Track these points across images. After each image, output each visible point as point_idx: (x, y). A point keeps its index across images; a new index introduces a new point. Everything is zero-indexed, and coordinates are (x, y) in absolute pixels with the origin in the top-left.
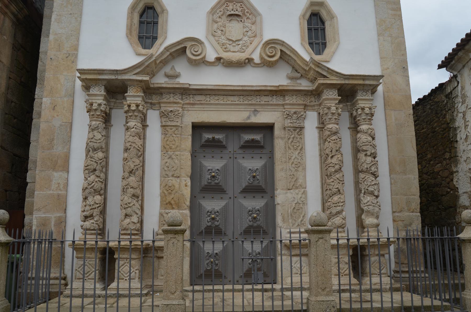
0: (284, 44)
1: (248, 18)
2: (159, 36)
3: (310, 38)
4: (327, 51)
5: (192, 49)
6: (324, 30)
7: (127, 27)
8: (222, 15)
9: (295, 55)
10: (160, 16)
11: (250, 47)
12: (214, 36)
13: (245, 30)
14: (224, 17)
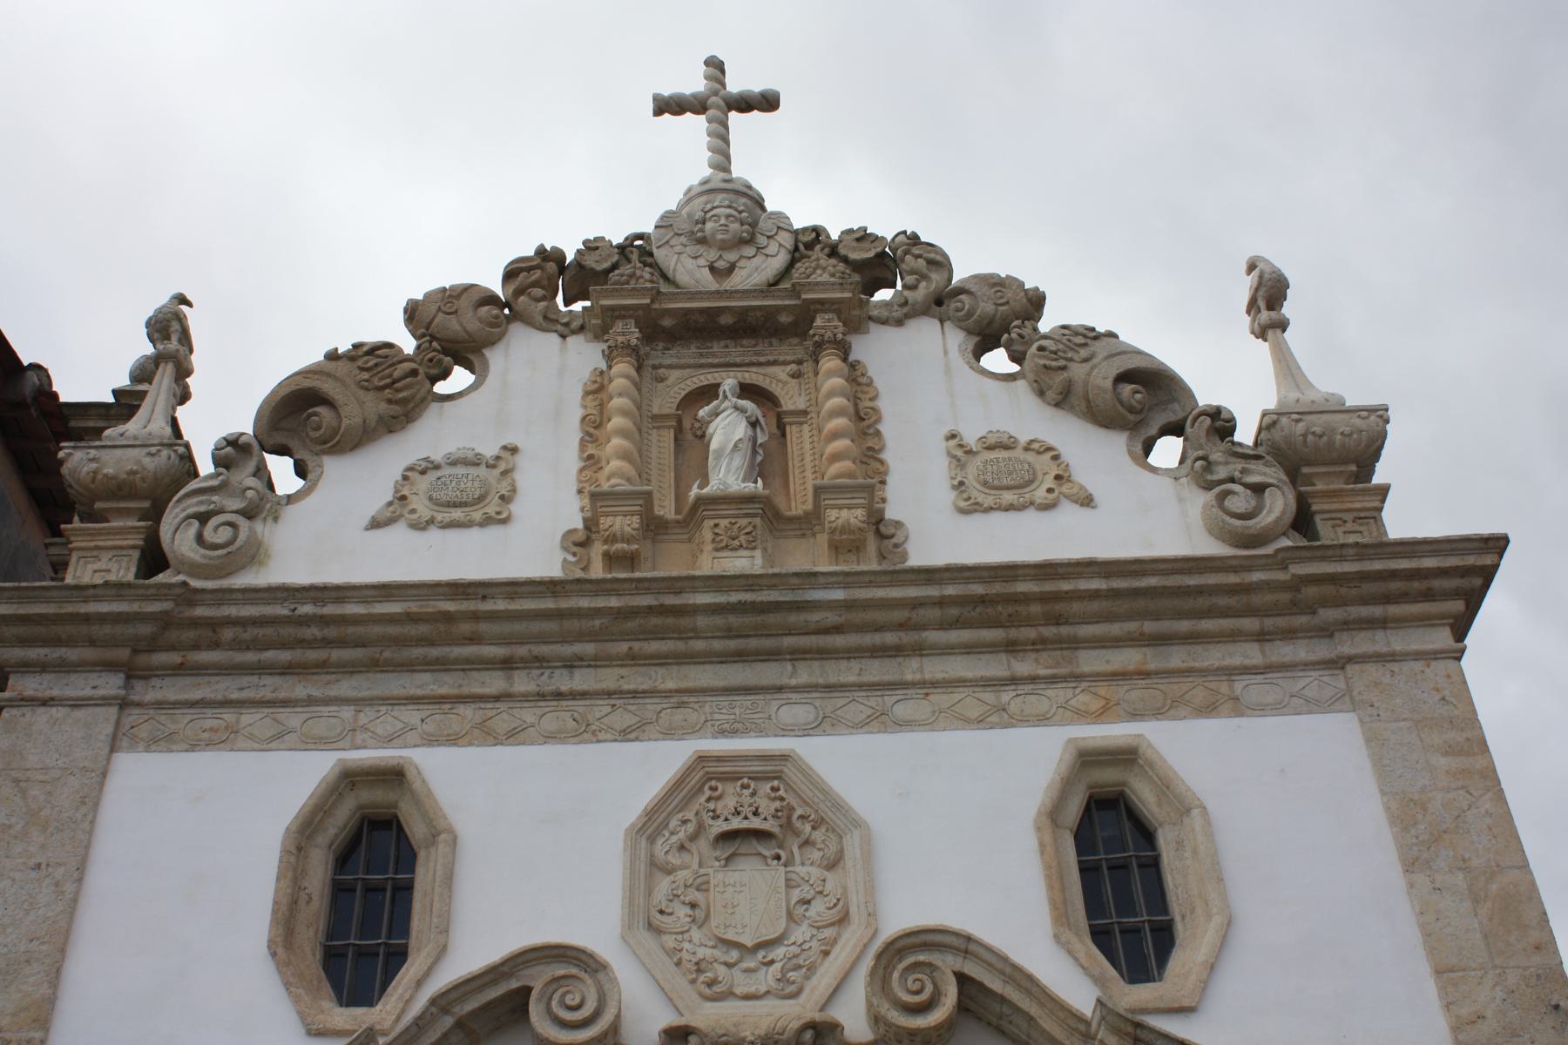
0: (972, 947)
1: (807, 843)
2: (413, 942)
3: (1093, 904)
4: (1179, 961)
5: (556, 997)
6: (1153, 866)
7: (274, 912)
8: (693, 838)
9: (1029, 992)
10: (422, 855)
11: (821, 970)
12: (656, 930)
13: (796, 895)
14: (703, 844)
